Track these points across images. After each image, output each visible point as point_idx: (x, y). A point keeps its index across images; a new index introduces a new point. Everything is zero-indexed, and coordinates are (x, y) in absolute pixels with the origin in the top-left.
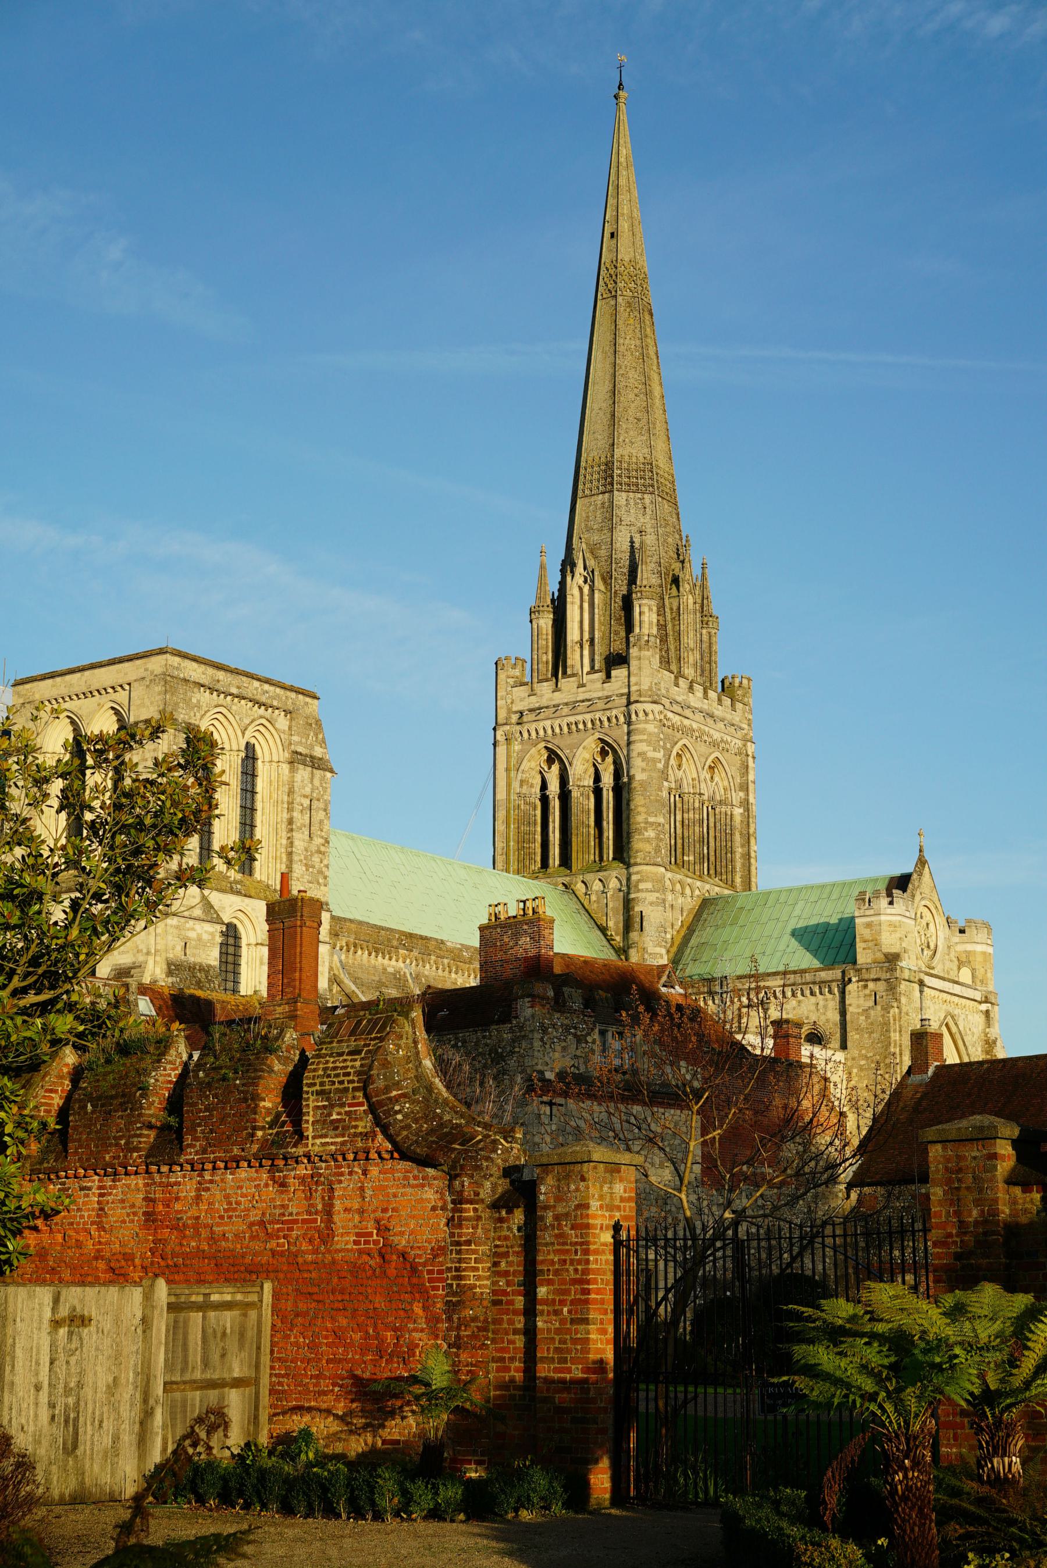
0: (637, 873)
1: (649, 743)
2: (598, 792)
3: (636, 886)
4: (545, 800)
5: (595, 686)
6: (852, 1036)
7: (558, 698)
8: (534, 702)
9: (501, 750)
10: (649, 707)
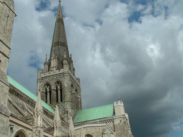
0: (66, 103)
1: (68, 80)
2: (57, 91)
3: (66, 105)
4: (46, 93)
5: (57, 72)
6: (116, 129)
7: (50, 75)
8: (45, 76)
9: (39, 84)
10: (68, 74)
